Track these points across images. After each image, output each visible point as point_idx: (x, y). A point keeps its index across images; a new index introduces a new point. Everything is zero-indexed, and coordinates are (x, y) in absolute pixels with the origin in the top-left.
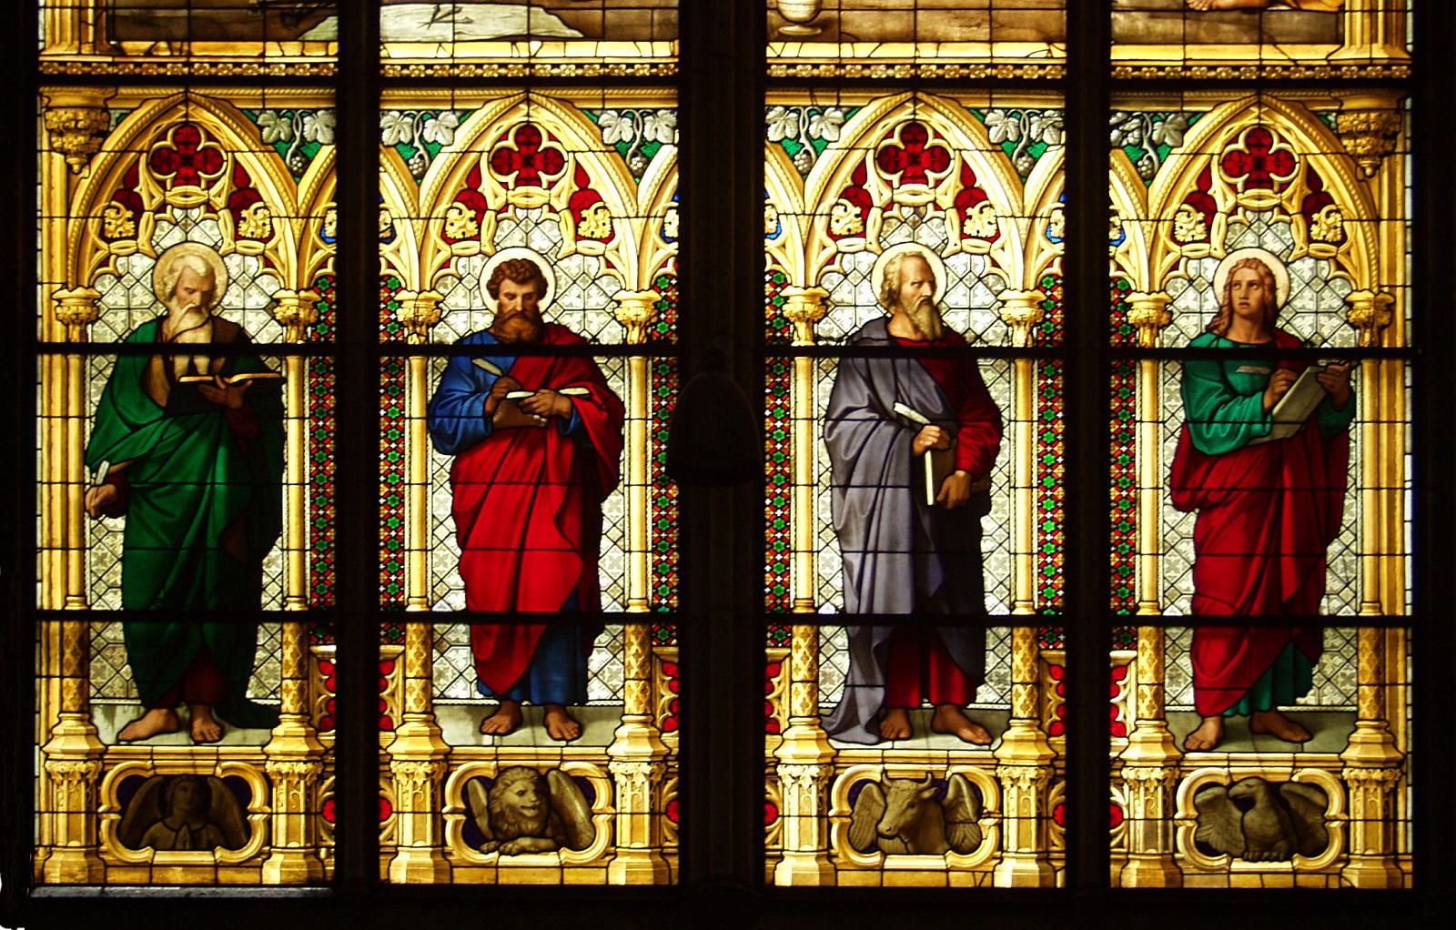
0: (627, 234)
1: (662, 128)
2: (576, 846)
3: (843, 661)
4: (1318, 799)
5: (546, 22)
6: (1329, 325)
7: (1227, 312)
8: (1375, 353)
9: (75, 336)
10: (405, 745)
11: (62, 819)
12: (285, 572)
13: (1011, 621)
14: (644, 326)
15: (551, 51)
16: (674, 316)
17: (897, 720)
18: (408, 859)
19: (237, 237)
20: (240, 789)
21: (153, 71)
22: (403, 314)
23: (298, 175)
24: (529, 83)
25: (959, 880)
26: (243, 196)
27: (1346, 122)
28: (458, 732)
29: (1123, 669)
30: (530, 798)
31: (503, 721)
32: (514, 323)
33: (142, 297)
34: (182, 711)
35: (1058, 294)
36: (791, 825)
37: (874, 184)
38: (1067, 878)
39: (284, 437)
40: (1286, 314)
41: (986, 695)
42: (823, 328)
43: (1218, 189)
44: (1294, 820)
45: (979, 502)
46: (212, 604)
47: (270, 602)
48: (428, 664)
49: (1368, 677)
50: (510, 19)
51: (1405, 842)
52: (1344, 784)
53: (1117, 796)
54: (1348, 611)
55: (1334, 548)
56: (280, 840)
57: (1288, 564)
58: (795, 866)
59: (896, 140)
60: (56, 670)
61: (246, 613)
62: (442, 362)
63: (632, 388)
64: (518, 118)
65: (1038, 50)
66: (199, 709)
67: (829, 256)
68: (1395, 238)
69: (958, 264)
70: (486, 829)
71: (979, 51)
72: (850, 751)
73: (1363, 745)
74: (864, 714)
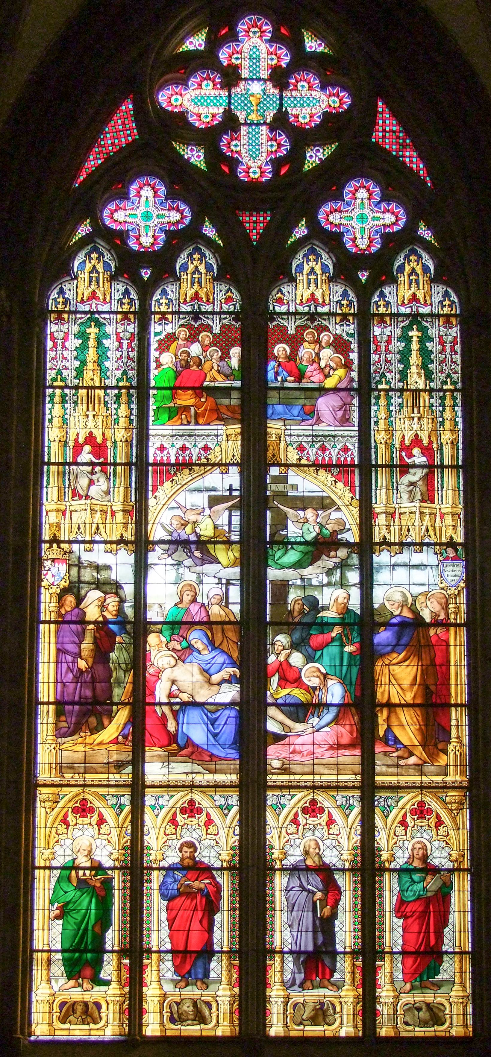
0: (222, 833)
1: (234, 800)
2: (205, 1023)
3: (291, 965)
4: (442, 1008)
5: (197, 768)
6: (444, 861)
7: (412, 857)
8: (459, 870)
9: (47, 865)
10: (151, 992)
11: (41, 1015)
12: (113, 938)
13: (345, 953)
14: (228, 861)
15: (199, 777)
16: (237, 858)
17: (308, 984)
18: (152, 1027)
19: (99, 834)
20: (98, 1005)
21: (74, 783)
22: (152, 858)
23: (119, 815)
24: (192, 786)
25: (328, 1034)
26: (101, 821)
27: (448, 799)
28: (168, 988)
29: (380, 967)
30: (191, 1008)
31: (183, 984)
32: (187, 860)
33: (69, 852)
34: (80, 981)
35: (359, 851)
36: (275, 1017)
37: (301, 818)
38: (363, 1033)
39: (113, 895)
40: (430, 858)
41: (336, 976)
42: (285, 862)
43: (409, 819)
44: (435, 1015)
45: (334, 915)
46: (90, 947)
47: (108, 947)
48: (159, 966)
49: (457, 969)
50: (186, 767)
51: (470, 1021)
52: (450, 1003)
53: (378, 1007)
54: (451, 950)
55: (446, 930)
56: (111, 1021)
57: (432, 936)
58: (276, 1029)
59: (308, 805)
60: (39, 968)
61: (100, 950)
62: (164, 872)
63: (224, 880)
64: (189, 797)
65: (352, 777)
66: (85, 980)
67: (286, 840)
68: (465, 835)
69: (328, 842)
70: (177, 1018)
71: (334, 778)
72: (293, 993)
73: (456, 991)
74: (298, 982)
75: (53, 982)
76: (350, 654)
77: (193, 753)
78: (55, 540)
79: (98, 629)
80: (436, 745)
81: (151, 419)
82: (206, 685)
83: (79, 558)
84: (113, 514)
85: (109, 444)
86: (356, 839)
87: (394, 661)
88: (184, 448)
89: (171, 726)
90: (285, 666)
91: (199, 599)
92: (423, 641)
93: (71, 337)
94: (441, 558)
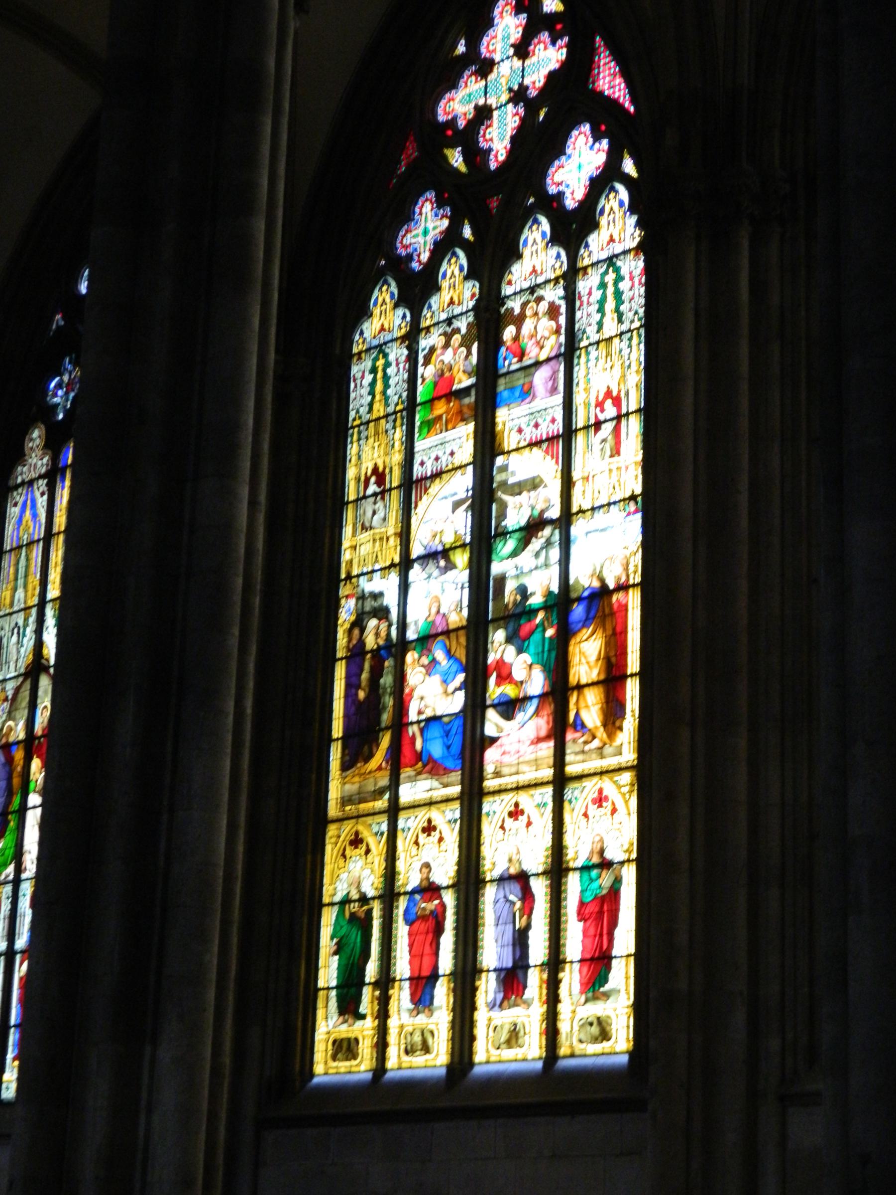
10: (393, 1023)
17: (506, 1003)
24: (430, 804)
33: (345, 886)
45: (528, 927)
74: (498, 1003)
75: (329, 1019)
76: (551, 638)
77: (432, 769)
78: (349, 577)
79: (373, 658)
80: (614, 723)
81: (417, 435)
82: (444, 696)
83: (363, 591)
84: (388, 539)
85: (387, 471)
86: (548, 840)
87: (585, 638)
88: (437, 459)
89: (419, 745)
90: (500, 663)
91: (442, 611)
92: (607, 611)
93: (367, 374)
94: (625, 514)
